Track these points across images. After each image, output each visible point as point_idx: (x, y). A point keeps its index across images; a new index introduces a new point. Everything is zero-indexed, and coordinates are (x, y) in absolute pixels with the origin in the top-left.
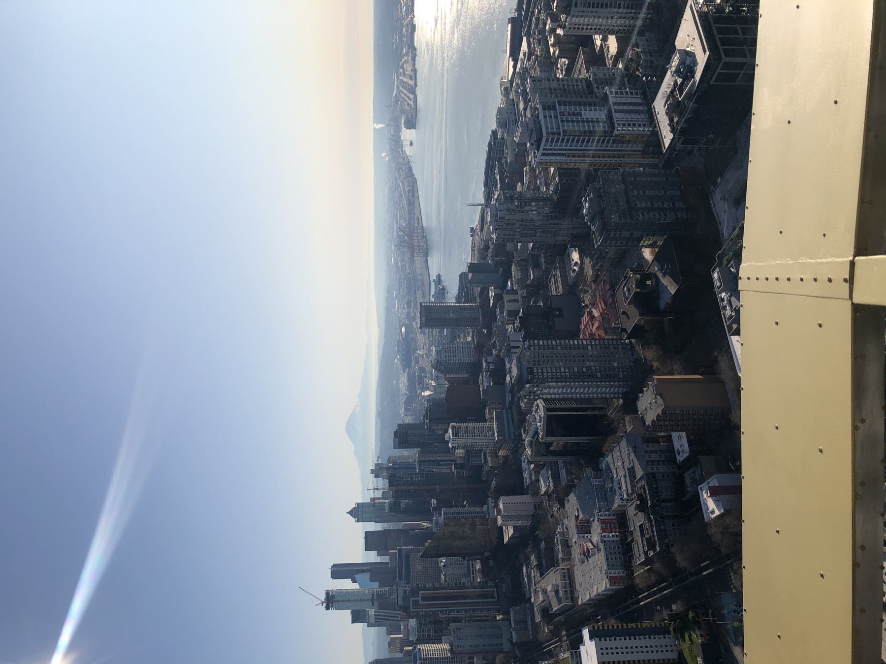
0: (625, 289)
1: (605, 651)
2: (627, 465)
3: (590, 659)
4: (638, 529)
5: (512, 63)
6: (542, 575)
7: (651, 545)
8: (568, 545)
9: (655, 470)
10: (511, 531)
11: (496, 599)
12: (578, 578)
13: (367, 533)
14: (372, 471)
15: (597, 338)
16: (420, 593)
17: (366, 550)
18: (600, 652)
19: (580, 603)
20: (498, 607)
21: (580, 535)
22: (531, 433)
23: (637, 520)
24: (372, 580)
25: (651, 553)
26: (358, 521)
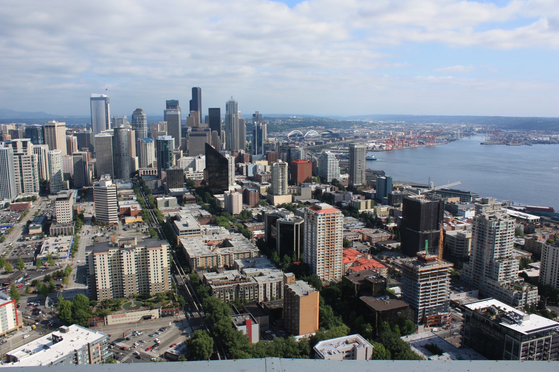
4: (225, 276)
5: (522, 208)
6: (196, 217)
13: (219, 109)
17: (210, 109)
19: (181, 239)
22: (282, 214)
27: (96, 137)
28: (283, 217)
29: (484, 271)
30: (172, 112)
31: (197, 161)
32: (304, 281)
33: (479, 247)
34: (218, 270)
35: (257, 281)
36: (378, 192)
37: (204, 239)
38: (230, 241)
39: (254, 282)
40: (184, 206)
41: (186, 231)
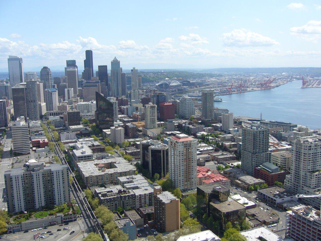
0: (220, 187)
2: (139, 186)
6: (89, 146)
7: (104, 195)
9: (137, 198)
12: (89, 163)
13: (106, 66)
14: (134, 68)
15: (197, 174)
17: (99, 66)
19: (78, 163)
21: (107, 165)
22: (153, 143)
23: (115, 189)
27: (12, 89)
28: (153, 145)
29: (301, 181)
30: (71, 69)
32: (169, 191)
33: (297, 164)
34: (106, 186)
36: (223, 125)
37: (95, 163)
38: (115, 164)
39: (132, 193)
40: (80, 139)
41: (82, 157)
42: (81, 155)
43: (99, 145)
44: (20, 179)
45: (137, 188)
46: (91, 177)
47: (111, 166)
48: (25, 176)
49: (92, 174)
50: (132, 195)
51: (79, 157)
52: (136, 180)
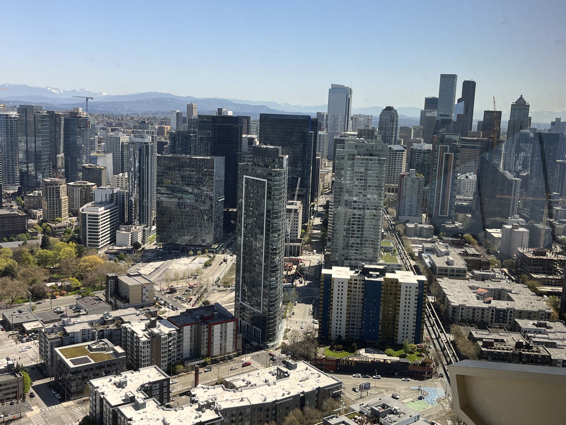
1: (408, 289)
2: (558, 342)
3: (403, 277)
7: (487, 344)
8: (483, 280)
10: (495, 235)
11: (439, 215)
12: (459, 282)
14: (558, 120)
16: (453, 154)
17: (485, 111)
18: (409, 286)
20: (433, 217)
21: (493, 292)
24: (458, 115)
25: (480, 344)
26: (512, 105)
31: (462, 182)
35: (549, 354)
37: (471, 285)
38: (509, 294)
41: (446, 270)
42: (446, 266)
43: (477, 255)
44: (346, 285)
45: (553, 345)
46: (462, 309)
47: (500, 295)
48: (353, 282)
49: (464, 303)
50: (545, 356)
51: (441, 269)
52: (552, 330)
